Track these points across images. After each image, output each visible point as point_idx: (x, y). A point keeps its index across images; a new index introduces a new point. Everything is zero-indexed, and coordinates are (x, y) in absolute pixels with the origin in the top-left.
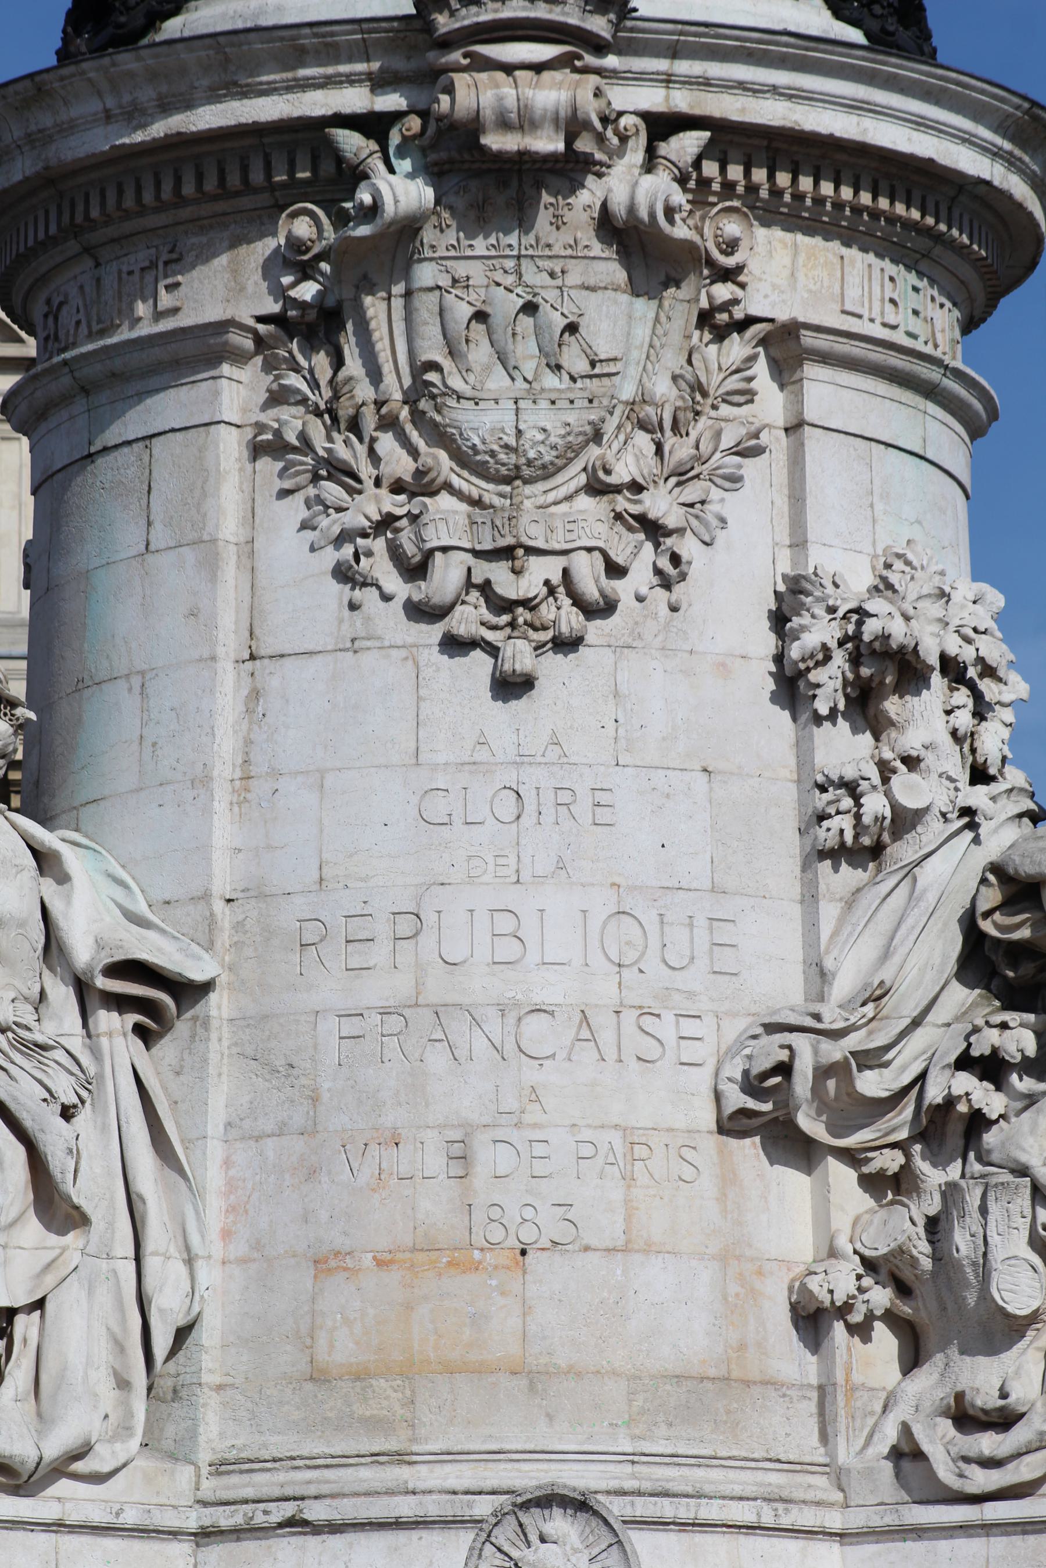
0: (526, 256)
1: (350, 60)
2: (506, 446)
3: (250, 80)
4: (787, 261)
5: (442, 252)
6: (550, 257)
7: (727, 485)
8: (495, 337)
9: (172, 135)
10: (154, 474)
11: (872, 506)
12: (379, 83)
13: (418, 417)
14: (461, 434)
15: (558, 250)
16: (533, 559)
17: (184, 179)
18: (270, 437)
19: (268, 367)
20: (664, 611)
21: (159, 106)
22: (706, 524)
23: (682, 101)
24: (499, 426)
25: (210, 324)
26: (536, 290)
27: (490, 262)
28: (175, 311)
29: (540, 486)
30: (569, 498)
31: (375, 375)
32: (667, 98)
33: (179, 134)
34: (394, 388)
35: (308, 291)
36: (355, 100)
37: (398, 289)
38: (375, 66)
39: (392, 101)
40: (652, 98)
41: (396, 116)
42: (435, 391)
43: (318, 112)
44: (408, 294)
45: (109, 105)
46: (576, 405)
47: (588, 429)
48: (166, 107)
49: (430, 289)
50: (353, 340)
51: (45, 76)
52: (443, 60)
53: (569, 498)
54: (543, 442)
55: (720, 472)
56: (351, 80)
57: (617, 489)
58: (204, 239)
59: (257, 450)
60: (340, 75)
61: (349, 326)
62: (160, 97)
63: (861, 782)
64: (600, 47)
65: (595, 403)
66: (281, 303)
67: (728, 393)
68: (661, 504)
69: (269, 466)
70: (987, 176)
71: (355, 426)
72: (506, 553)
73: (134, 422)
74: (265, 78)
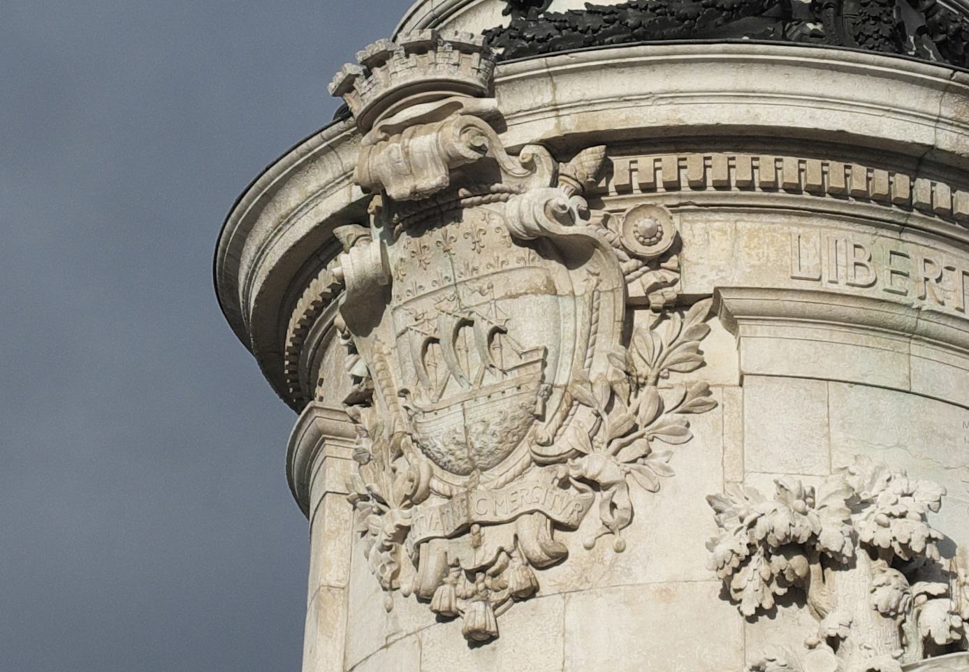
0: (460, 283)
2: (458, 443)
4: (726, 245)
6: (478, 279)
7: (673, 439)
11: (828, 436)
15: (483, 271)
16: (485, 530)
20: (609, 554)
22: (648, 476)
23: (571, 124)
24: (452, 428)
26: (471, 309)
29: (496, 471)
30: (521, 473)
32: (558, 125)
40: (547, 128)
46: (507, 395)
47: (520, 412)
53: (521, 473)
54: (484, 432)
55: (664, 429)
57: (561, 460)
63: (768, 664)
64: (480, 95)
65: (523, 390)
67: (673, 364)
68: (598, 464)
70: (929, 142)
72: (464, 530)
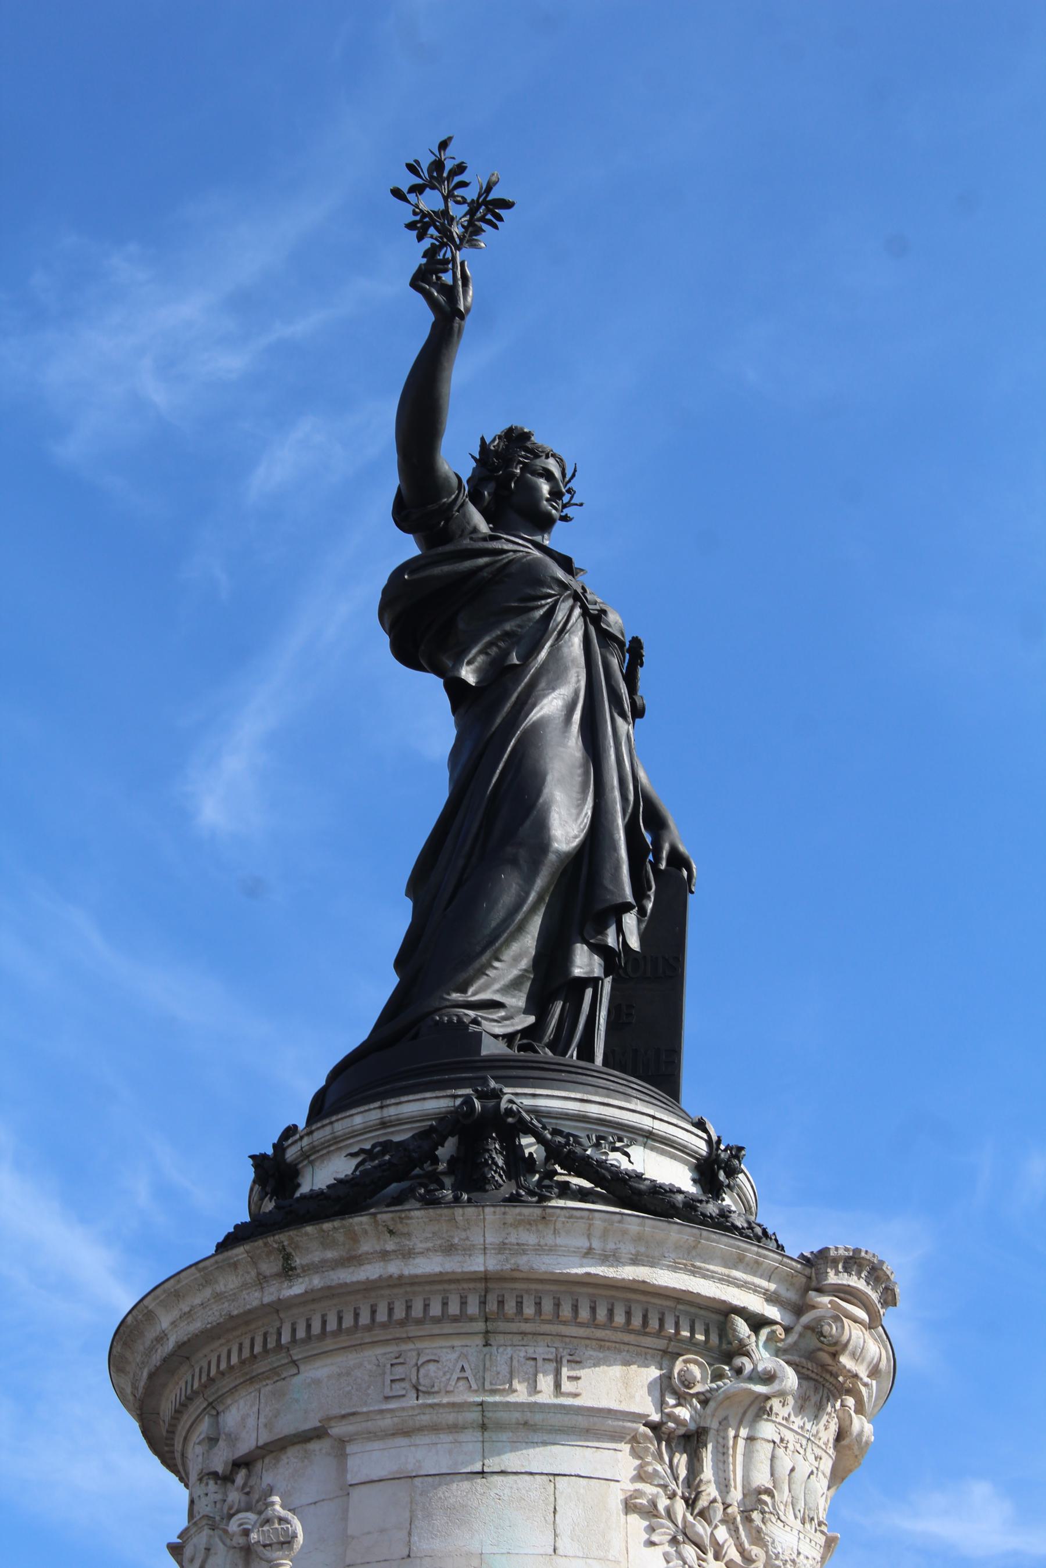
1: (761, 1277)
3: (703, 1265)
5: (779, 1420)
8: (793, 1486)
9: (638, 1281)
10: (559, 1501)
12: (771, 1298)
13: (748, 1520)
14: (773, 1542)
17: (615, 1311)
18: (644, 1502)
19: (635, 1453)
21: (631, 1259)
25: (634, 1413)
27: (797, 1437)
28: (576, 1395)
31: (724, 1486)
33: (644, 1282)
34: (736, 1495)
35: (684, 1413)
36: (756, 1304)
37: (744, 1432)
38: (772, 1287)
39: (773, 1312)
41: (776, 1323)
42: (766, 1509)
43: (736, 1302)
44: (751, 1439)
45: (594, 1246)
48: (635, 1261)
49: (769, 1441)
50: (710, 1456)
51: (558, 1211)
52: (819, 1299)
56: (755, 1289)
58: (601, 1355)
59: (630, 1506)
60: (753, 1284)
61: (710, 1446)
62: (637, 1254)
66: (659, 1415)
69: (637, 1523)
71: (702, 1514)
73: (512, 1460)
74: (711, 1267)
